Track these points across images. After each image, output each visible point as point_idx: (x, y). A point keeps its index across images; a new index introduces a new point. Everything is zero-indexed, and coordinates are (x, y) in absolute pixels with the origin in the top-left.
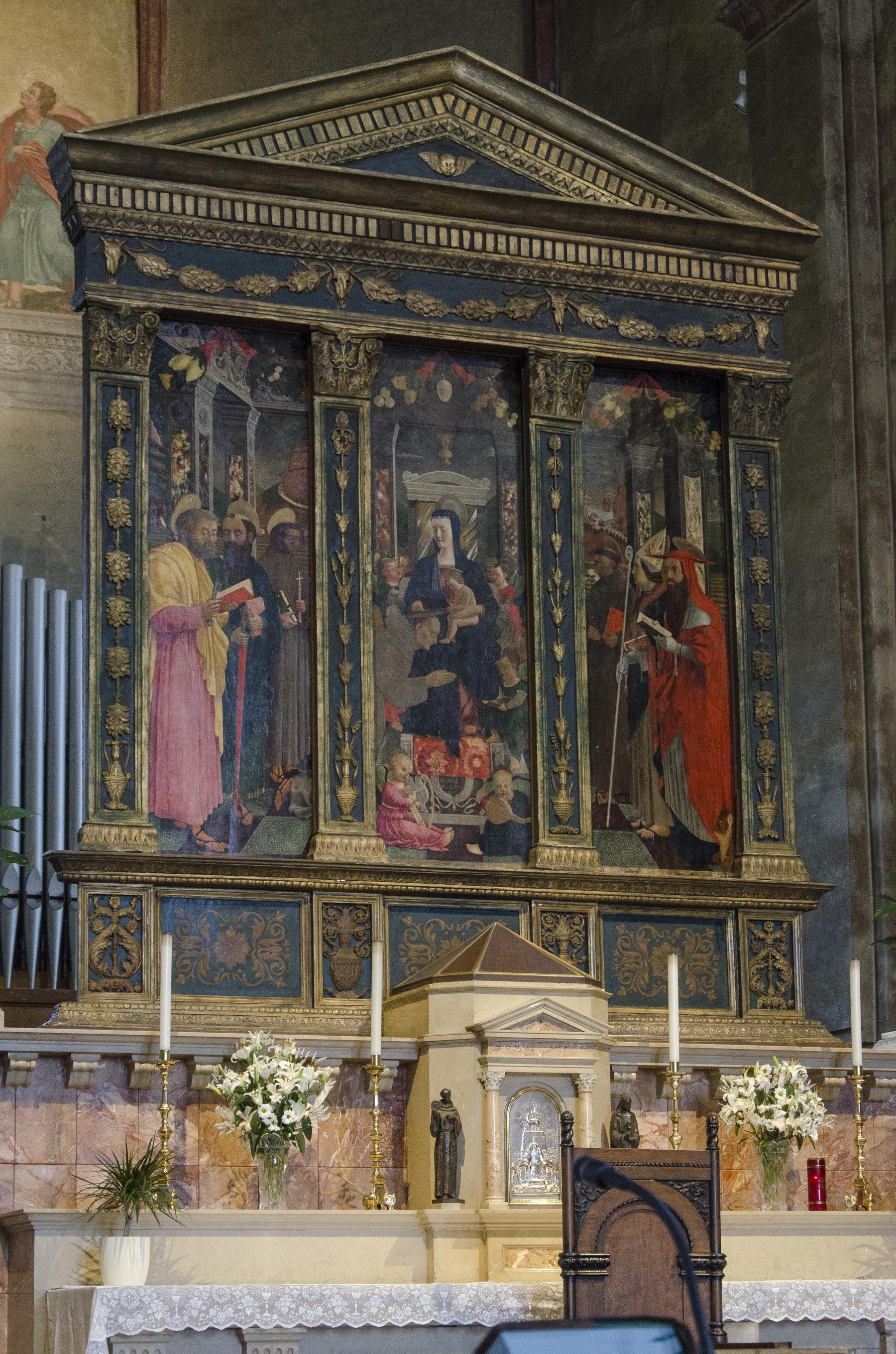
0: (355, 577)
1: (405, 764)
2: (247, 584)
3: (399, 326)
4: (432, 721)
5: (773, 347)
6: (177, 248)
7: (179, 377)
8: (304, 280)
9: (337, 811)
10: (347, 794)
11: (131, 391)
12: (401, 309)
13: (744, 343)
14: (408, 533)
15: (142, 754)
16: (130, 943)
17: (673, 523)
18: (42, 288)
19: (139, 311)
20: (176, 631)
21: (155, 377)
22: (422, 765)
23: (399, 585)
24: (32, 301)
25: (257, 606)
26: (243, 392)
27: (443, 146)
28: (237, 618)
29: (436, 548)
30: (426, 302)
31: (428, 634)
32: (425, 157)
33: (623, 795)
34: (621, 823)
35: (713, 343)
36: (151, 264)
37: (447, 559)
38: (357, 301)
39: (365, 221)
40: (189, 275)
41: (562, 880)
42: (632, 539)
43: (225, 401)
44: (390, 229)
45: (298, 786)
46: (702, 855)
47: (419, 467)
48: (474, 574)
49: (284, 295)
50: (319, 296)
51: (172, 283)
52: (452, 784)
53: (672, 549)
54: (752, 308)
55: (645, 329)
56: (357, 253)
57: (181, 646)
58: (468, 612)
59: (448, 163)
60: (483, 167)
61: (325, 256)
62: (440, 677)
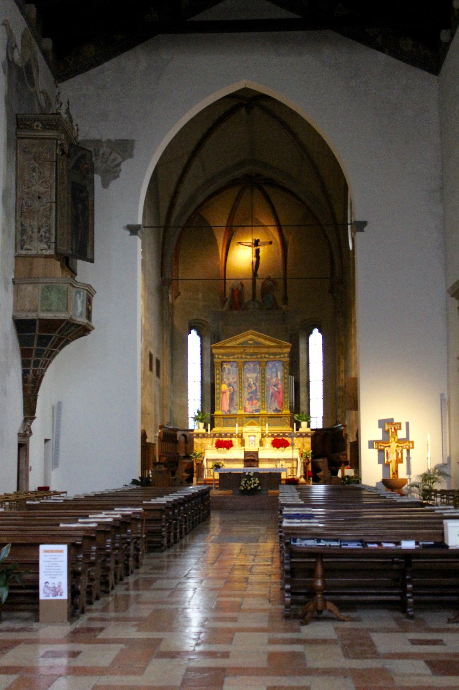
0: (242, 386)
1: (247, 404)
2: (231, 387)
3: (246, 360)
4: (250, 399)
5: (287, 357)
6: (223, 354)
7: (224, 368)
8: (236, 356)
9: (240, 409)
10: (241, 407)
11: (219, 370)
12: (246, 358)
13: (284, 357)
14: (248, 380)
15: (220, 405)
16: (220, 423)
17: (277, 376)
18: (269, 307)
19: (219, 362)
20: (224, 393)
21: (221, 368)
22: (249, 404)
23: (247, 386)
24: (268, 309)
25: (232, 389)
26: (230, 368)
27: (251, 340)
28: (230, 390)
29: (251, 382)
30: (249, 357)
31: (250, 391)
32: (249, 342)
33: (270, 405)
34: (270, 408)
35: (280, 358)
36: (220, 357)
37: (252, 383)
38: (242, 358)
39: (242, 350)
40: (225, 357)
41: (263, 415)
42: (272, 379)
43: (229, 369)
44: (245, 350)
45: (236, 407)
46: (279, 411)
47: (249, 373)
48: (254, 384)
49: (234, 358)
50: (238, 358)
51: (222, 358)
52: (252, 405)
53: (276, 379)
54: (285, 353)
55: (273, 357)
56: (241, 353)
57: (224, 394)
58: (254, 388)
59: (251, 342)
60: (255, 342)
61: (238, 353)
62: (251, 395)
